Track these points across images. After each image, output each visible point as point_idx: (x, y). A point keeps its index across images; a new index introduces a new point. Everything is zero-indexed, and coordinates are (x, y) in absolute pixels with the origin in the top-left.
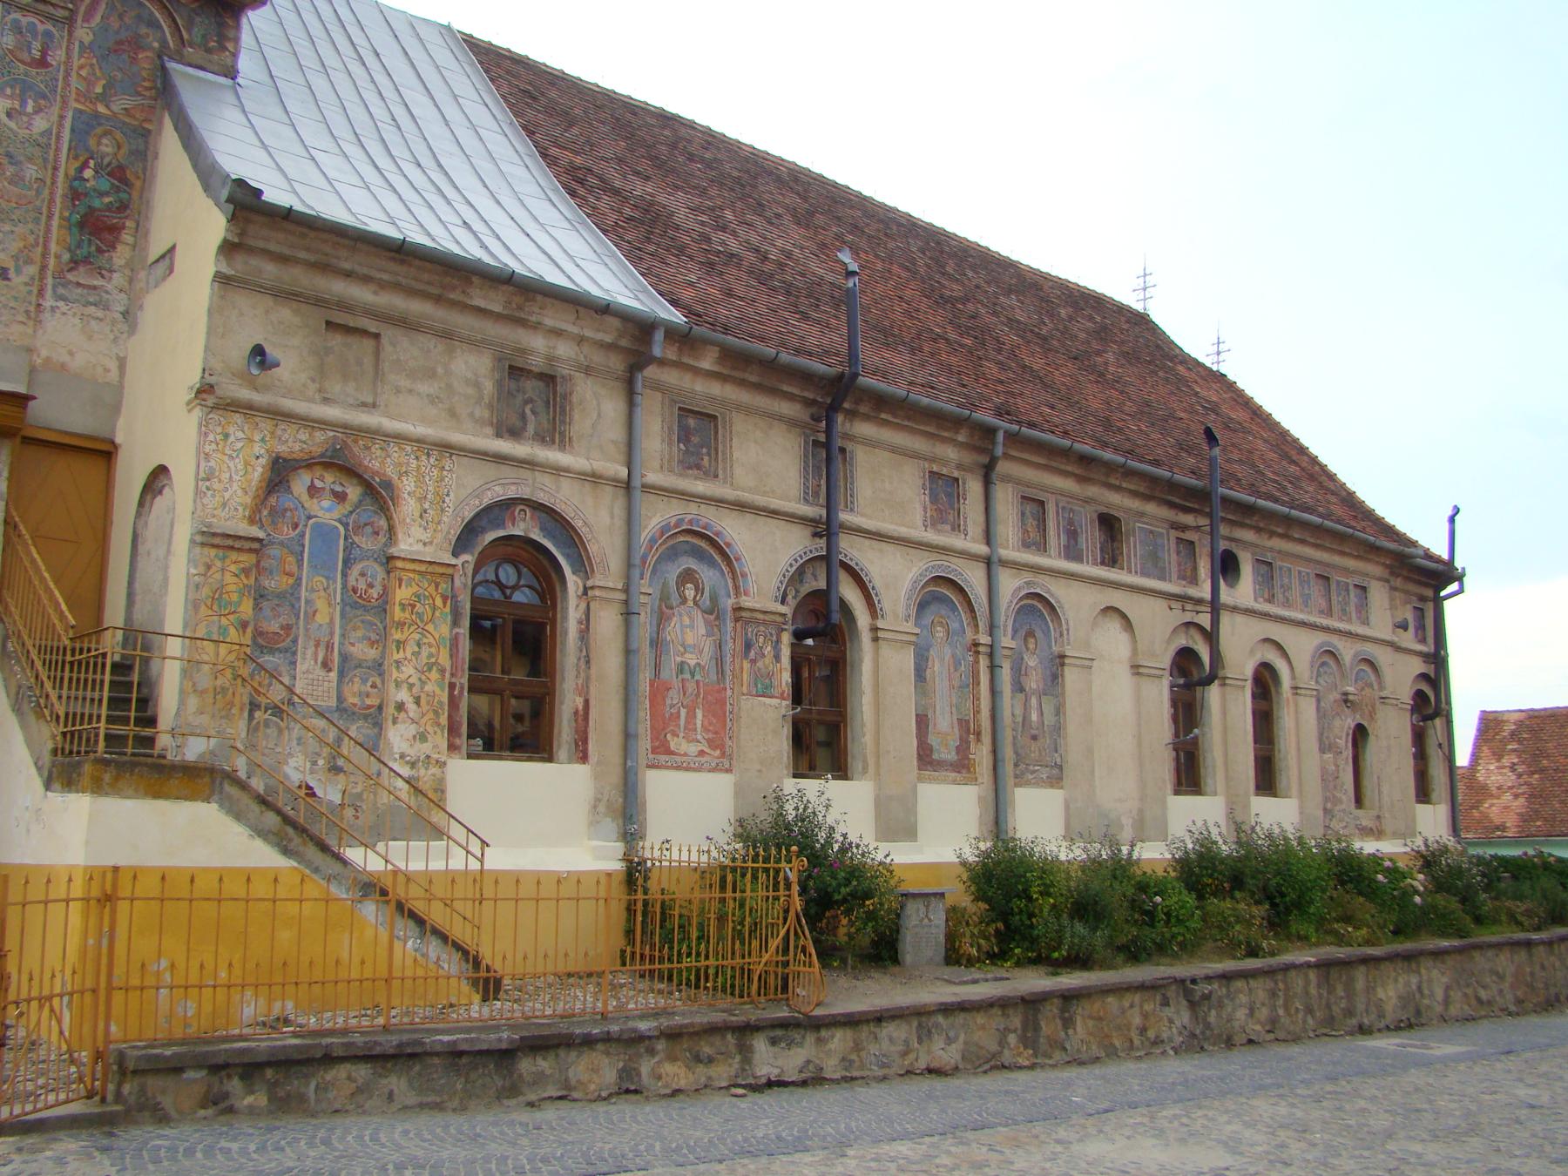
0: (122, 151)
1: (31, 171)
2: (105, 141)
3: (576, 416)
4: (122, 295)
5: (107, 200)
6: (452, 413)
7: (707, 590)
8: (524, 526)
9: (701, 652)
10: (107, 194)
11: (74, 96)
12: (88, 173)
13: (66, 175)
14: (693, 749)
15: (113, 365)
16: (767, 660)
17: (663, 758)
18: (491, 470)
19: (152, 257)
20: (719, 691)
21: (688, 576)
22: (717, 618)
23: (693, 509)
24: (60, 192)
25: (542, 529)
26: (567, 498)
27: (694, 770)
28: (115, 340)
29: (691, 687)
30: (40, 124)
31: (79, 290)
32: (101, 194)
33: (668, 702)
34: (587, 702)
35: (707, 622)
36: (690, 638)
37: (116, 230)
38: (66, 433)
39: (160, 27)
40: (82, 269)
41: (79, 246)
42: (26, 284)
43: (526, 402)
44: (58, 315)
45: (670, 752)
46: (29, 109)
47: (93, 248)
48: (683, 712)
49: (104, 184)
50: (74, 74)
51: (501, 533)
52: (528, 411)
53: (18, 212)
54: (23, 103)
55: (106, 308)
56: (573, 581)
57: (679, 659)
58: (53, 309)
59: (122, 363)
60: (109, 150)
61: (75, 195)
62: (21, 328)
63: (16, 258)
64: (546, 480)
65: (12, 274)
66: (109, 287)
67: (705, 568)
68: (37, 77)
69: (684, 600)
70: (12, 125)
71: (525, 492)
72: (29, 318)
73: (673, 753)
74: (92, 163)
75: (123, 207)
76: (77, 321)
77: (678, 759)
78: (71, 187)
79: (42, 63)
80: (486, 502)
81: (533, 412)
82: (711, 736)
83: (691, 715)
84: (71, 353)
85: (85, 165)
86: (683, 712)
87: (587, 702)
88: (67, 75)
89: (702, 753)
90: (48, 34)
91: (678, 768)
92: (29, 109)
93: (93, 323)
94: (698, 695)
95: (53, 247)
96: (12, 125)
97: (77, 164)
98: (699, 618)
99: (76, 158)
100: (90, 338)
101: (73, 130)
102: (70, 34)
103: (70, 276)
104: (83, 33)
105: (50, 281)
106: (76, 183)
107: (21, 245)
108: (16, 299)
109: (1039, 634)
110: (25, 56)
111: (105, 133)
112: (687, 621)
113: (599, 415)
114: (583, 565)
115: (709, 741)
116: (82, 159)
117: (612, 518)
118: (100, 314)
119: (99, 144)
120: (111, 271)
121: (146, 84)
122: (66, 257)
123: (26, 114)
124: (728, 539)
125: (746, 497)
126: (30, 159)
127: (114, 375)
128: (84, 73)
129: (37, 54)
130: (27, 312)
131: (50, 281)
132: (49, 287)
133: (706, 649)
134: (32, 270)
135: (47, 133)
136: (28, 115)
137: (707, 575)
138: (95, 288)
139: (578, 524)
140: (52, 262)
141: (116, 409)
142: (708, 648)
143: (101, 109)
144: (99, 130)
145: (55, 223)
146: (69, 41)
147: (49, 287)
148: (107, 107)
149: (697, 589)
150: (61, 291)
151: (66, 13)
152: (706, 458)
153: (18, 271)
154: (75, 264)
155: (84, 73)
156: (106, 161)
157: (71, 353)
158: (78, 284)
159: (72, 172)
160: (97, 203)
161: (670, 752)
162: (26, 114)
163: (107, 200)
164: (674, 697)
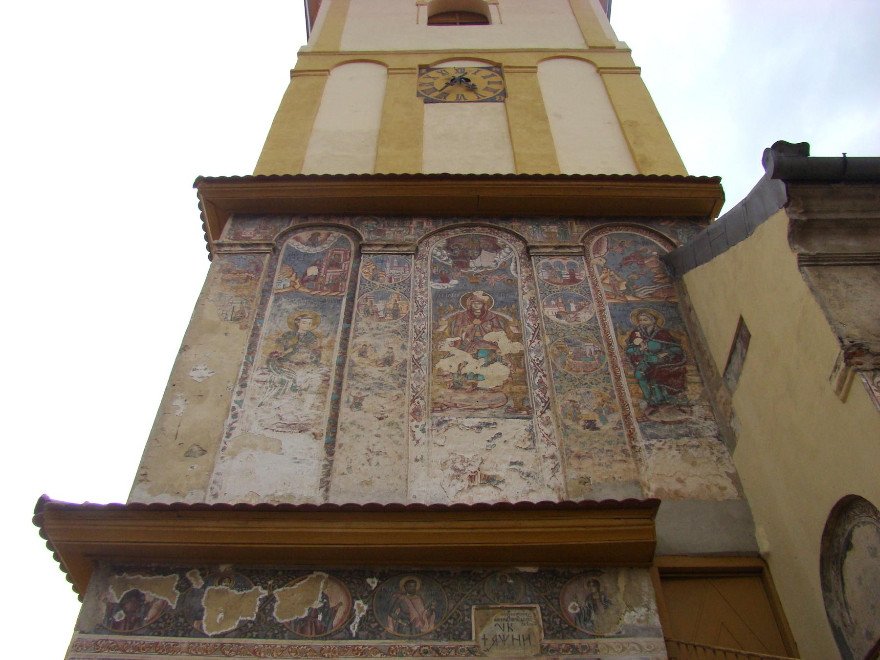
0: (660, 321)
1: (589, 348)
2: (642, 317)
4: (709, 422)
5: (662, 355)
10: (661, 351)
11: (604, 296)
12: (638, 341)
13: (620, 346)
15: (727, 483)
19: (721, 371)
24: (619, 359)
28: (719, 459)
30: (585, 316)
31: (667, 427)
32: (656, 353)
37: (681, 375)
38: (705, 556)
39: (654, 243)
40: (662, 410)
41: (651, 393)
42: (615, 429)
44: (654, 451)
46: (573, 308)
47: (666, 393)
49: (655, 345)
50: (600, 284)
53: (588, 378)
54: (567, 306)
55: (698, 435)
58: (648, 447)
59: (735, 479)
60: (648, 322)
61: (633, 359)
62: (624, 466)
63: (598, 411)
65: (599, 424)
66: (694, 418)
68: (574, 290)
70: (563, 321)
72: (628, 455)
74: (638, 334)
75: (678, 357)
76: (674, 452)
78: (627, 354)
79: (573, 280)
84: (680, 481)
85: (632, 337)
88: (595, 286)
90: (569, 264)
92: (573, 308)
93: (691, 451)
95: (629, 399)
96: (563, 321)
97: (626, 338)
99: (623, 334)
100: (694, 464)
101: (613, 317)
102: (588, 263)
103: (653, 418)
104: (596, 260)
105: (636, 426)
106: (631, 350)
107: (600, 400)
108: (610, 443)
110: (559, 280)
111: (640, 313)
116: (628, 333)
118: (695, 442)
119: (638, 320)
120: (691, 406)
121: (659, 276)
122: (644, 404)
123: (571, 313)
126: (586, 340)
127: (731, 491)
128: (607, 281)
129: (568, 277)
130: (624, 451)
131: (636, 426)
132: (638, 430)
134: (617, 416)
135: (594, 319)
136: (573, 313)
138: (680, 422)
140: (632, 410)
141: (749, 522)
143: (630, 298)
144: (635, 311)
145: (624, 381)
146: (588, 266)
147: (638, 430)
148: (634, 296)
150: (649, 431)
151: (580, 250)
153: (605, 421)
154: (654, 408)
155: (607, 281)
156: (649, 330)
157: (680, 481)
158: (664, 423)
159: (624, 344)
160: (654, 360)
162: (571, 313)
163: (662, 355)
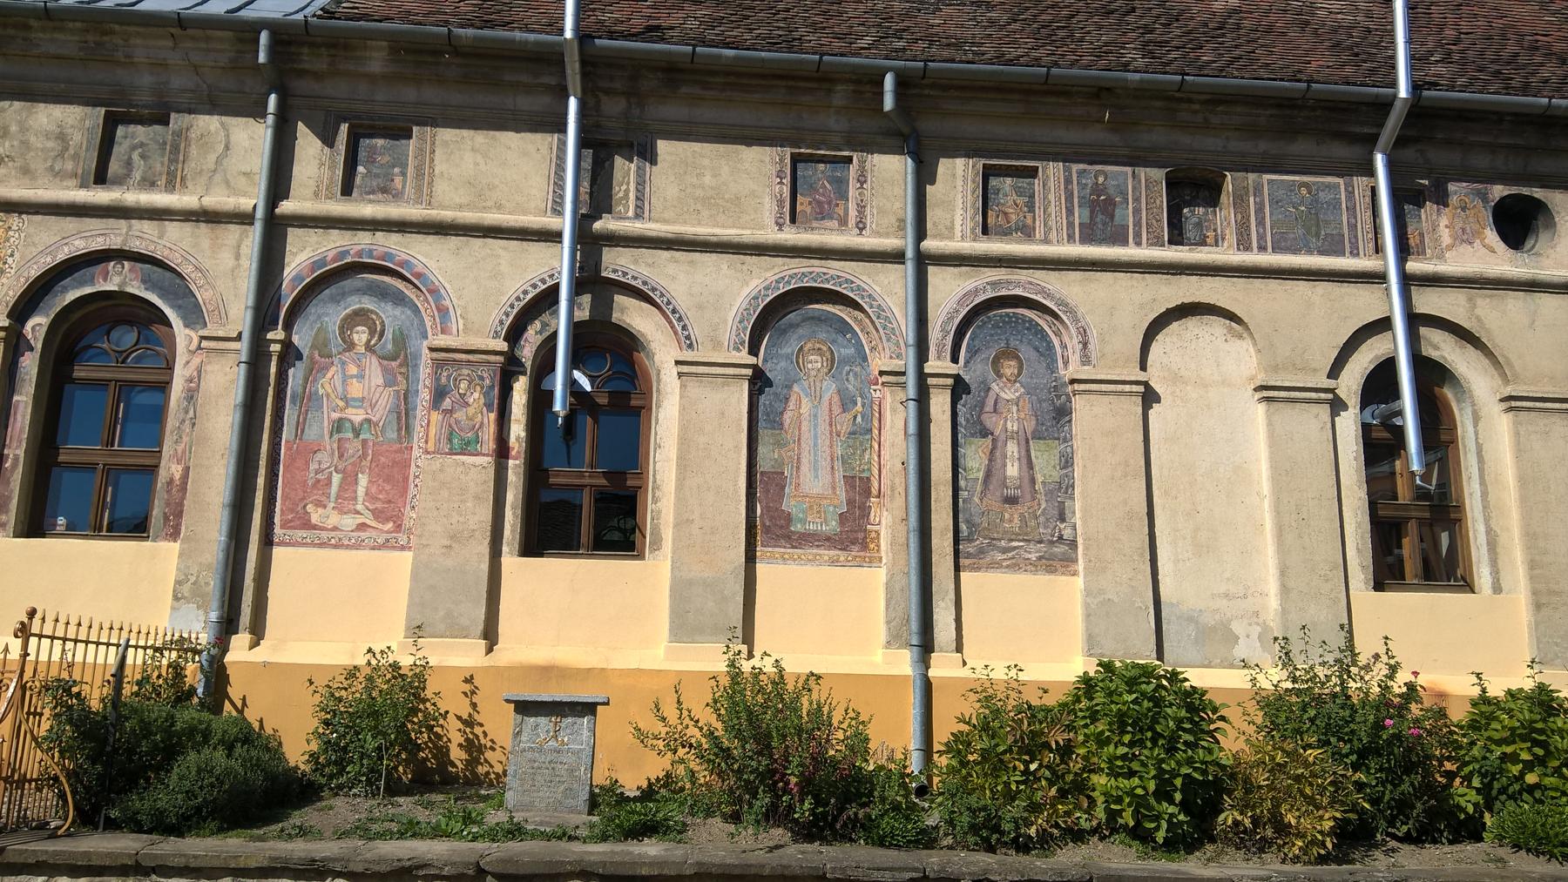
3: (194, 151)
6: (26, 171)
7: (389, 335)
8: (115, 279)
9: (372, 407)
14: (349, 522)
16: (471, 411)
17: (303, 533)
18: (70, 224)
20: (399, 451)
21: (360, 317)
22: (405, 363)
23: (364, 239)
25: (144, 281)
26: (171, 242)
27: (348, 547)
29: (353, 447)
33: (313, 466)
34: (187, 470)
35: (385, 370)
36: (356, 389)
43: (134, 148)
45: (307, 525)
48: (336, 478)
51: (88, 290)
52: (135, 156)
56: (183, 335)
57: (335, 416)
64: (147, 227)
67: (389, 307)
69: (350, 346)
71: (115, 242)
73: (315, 527)
77: (324, 534)
80: (61, 257)
81: (142, 156)
82: (379, 505)
83: (350, 480)
86: (336, 478)
87: (187, 470)
89: (362, 527)
91: (322, 545)
94: (364, 455)
98: (374, 368)
109: (1026, 352)
112: (353, 370)
113: (227, 148)
114: (194, 315)
115: (373, 511)
117: (238, 257)
124: (420, 268)
125: (447, 215)
133: (383, 402)
137: (389, 315)
139: (186, 270)
142: (385, 400)
149: (372, 332)
152: (398, 180)
161: (307, 525)
164: (324, 459)
